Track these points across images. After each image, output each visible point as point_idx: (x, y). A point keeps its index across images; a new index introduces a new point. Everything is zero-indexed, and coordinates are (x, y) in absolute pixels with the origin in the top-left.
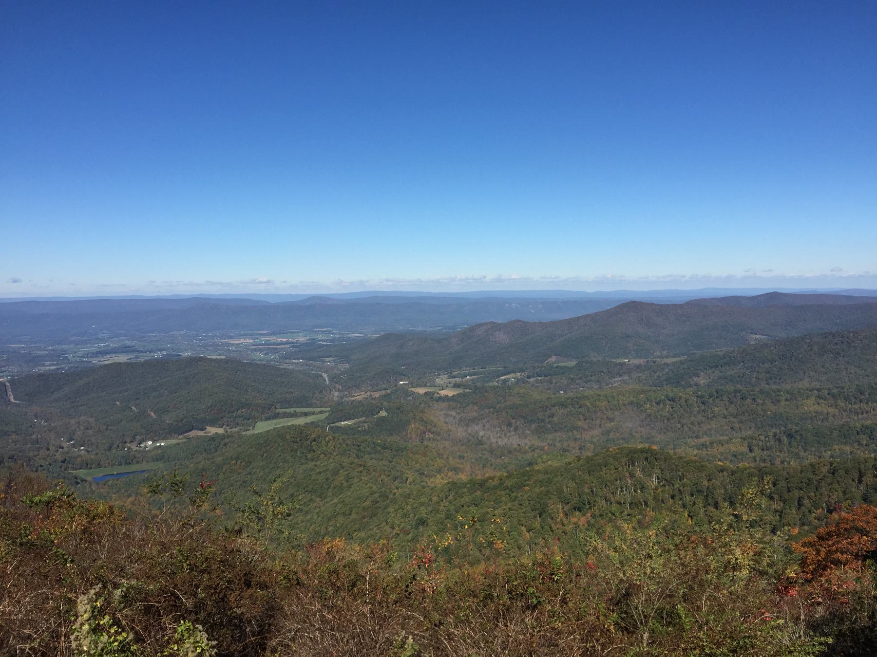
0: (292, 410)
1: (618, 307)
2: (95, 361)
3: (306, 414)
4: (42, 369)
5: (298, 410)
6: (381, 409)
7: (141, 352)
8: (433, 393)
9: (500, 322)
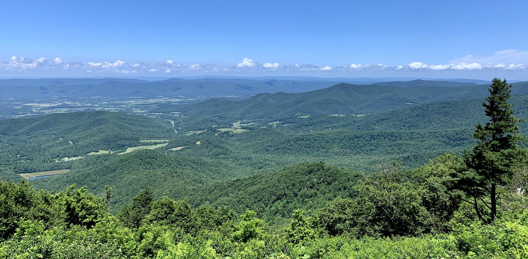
0: (148, 141)
1: (334, 86)
2: (47, 112)
3: (156, 144)
4: (17, 117)
5: (152, 141)
6: (198, 141)
7: (71, 107)
8: (229, 132)
9: (273, 93)
